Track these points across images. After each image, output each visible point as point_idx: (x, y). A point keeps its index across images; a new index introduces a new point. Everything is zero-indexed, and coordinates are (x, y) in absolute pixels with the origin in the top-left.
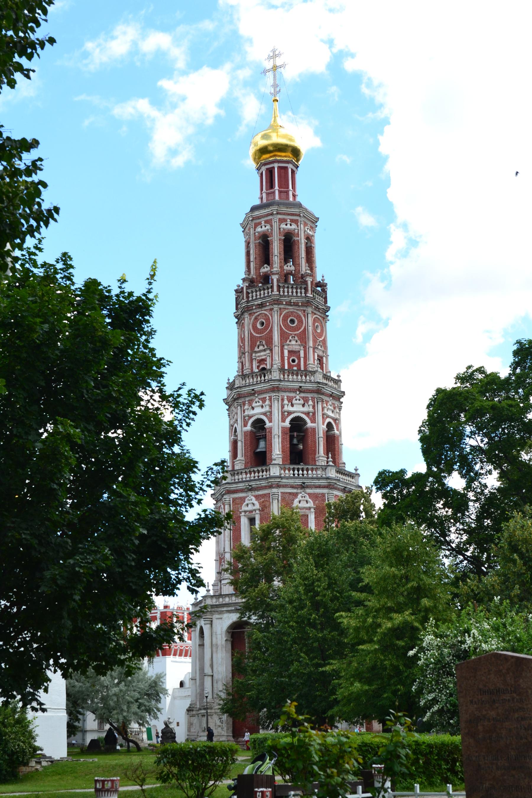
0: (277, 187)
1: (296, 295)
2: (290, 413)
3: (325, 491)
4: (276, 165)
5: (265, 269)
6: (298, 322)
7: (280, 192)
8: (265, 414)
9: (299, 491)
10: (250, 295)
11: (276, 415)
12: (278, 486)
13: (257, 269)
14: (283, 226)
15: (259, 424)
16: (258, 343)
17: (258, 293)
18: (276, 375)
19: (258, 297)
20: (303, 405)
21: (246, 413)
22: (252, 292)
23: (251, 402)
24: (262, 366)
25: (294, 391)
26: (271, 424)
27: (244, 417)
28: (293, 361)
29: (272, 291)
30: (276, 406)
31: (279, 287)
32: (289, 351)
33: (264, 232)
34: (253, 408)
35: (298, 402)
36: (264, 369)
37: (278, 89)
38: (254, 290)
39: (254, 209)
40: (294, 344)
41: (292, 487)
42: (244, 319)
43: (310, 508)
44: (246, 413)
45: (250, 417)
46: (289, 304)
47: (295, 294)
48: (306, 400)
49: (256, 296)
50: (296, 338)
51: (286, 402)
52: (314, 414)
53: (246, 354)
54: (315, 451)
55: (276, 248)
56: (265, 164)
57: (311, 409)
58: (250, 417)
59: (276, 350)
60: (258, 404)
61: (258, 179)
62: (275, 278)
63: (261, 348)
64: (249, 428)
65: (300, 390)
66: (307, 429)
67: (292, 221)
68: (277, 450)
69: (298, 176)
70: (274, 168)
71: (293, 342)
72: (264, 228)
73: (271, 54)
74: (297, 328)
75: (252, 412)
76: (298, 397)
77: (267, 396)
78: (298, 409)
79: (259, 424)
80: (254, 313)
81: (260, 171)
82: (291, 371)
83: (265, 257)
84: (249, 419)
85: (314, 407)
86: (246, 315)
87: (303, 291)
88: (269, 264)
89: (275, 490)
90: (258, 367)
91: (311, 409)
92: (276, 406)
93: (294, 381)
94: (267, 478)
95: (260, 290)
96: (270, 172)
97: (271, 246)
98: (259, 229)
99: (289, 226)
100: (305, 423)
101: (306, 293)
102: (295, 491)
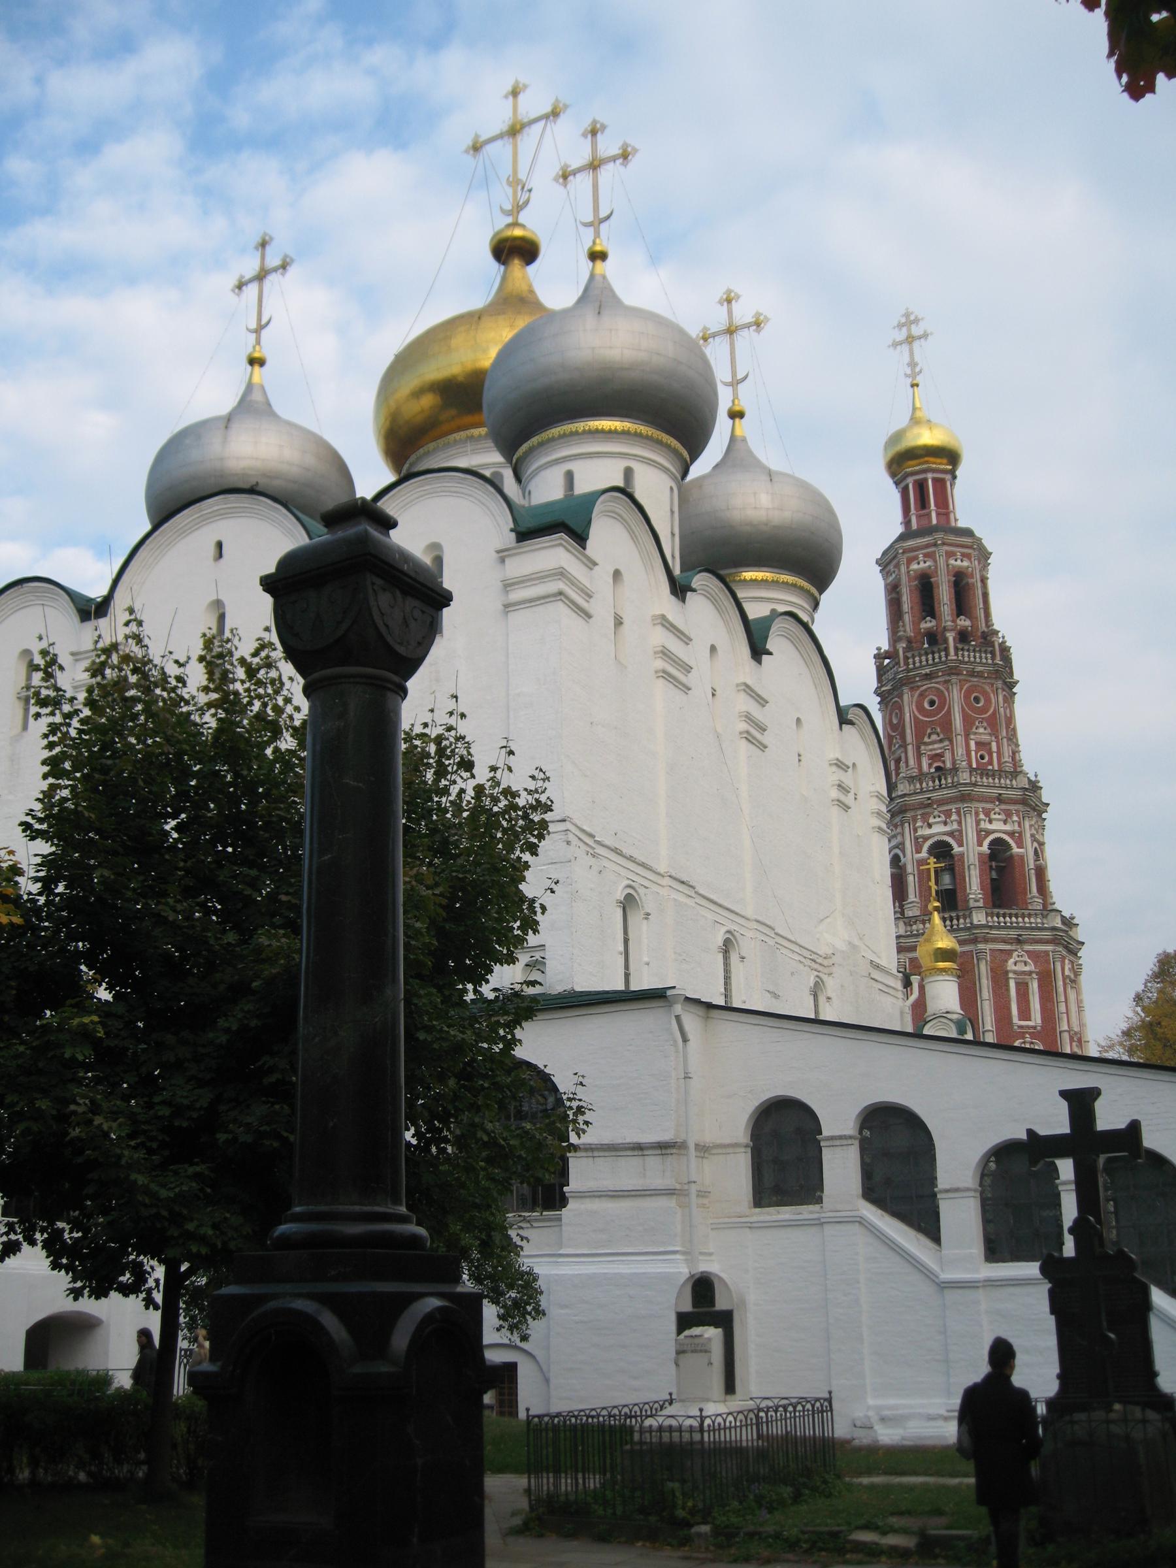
0: (933, 506)
1: (982, 661)
2: (989, 832)
3: (1049, 948)
4: (930, 476)
5: (928, 624)
6: (986, 701)
7: (938, 514)
8: (951, 834)
9: (1013, 948)
10: (911, 661)
11: (971, 835)
12: (986, 941)
13: (916, 624)
14: (952, 562)
15: (941, 850)
16: (929, 731)
17: (924, 658)
18: (964, 777)
19: (924, 663)
20: (1005, 822)
21: (920, 833)
22: (913, 656)
23: (925, 818)
24: (936, 765)
25: (990, 800)
26: (961, 849)
27: (916, 838)
28: (982, 757)
29: (947, 655)
30: (970, 822)
31: (956, 649)
32: (977, 743)
33: (922, 570)
34: (930, 826)
35: (997, 816)
36: (938, 769)
37: (917, 369)
38: (916, 653)
39: (902, 538)
40: (982, 732)
41: (1005, 941)
42: (901, 696)
43: (1030, 973)
44: (920, 833)
46: (972, 674)
47: (978, 660)
48: (1008, 814)
49: (921, 662)
50: (985, 724)
51: (982, 816)
52: (1020, 833)
53: (910, 747)
54: (1025, 889)
55: (944, 595)
57: (1016, 828)
58: (926, 838)
59: (960, 740)
60: (938, 819)
61: (895, 496)
62: (950, 636)
63: (934, 737)
65: (1000, 799)
66: (1012, 857)
67: (963, 555)
68: (974, 886)
69: (955, 491)
70: (926, 480)
71: (981, 730)
72: (922, 565)
73: (903, 320)
74: (984, 710)
75: (927, 832)
76: (997, 810)
77: (953, 807)
78: (998, 827)
79: (941, 850)
80: (919, 687)
81: (903, 485)
82: (983, 771)
83: (927, 605)
84: (924, 842)
85: (1020, 826)
86: (906, 690)
87: (989, 656)
88: (933, 616)
89: (981, 946)
90: (930, 765)
91: (1016, 828)
92: (970, 822)
93: (988, 787)
94: (968, 929)
95: (927, 654)
96: (921, 487)
97: (935, 591)
98: (914, 566)
99: (959, 562)
100: (1009, 847)
101: (993, 658)
102: (1008, 947)
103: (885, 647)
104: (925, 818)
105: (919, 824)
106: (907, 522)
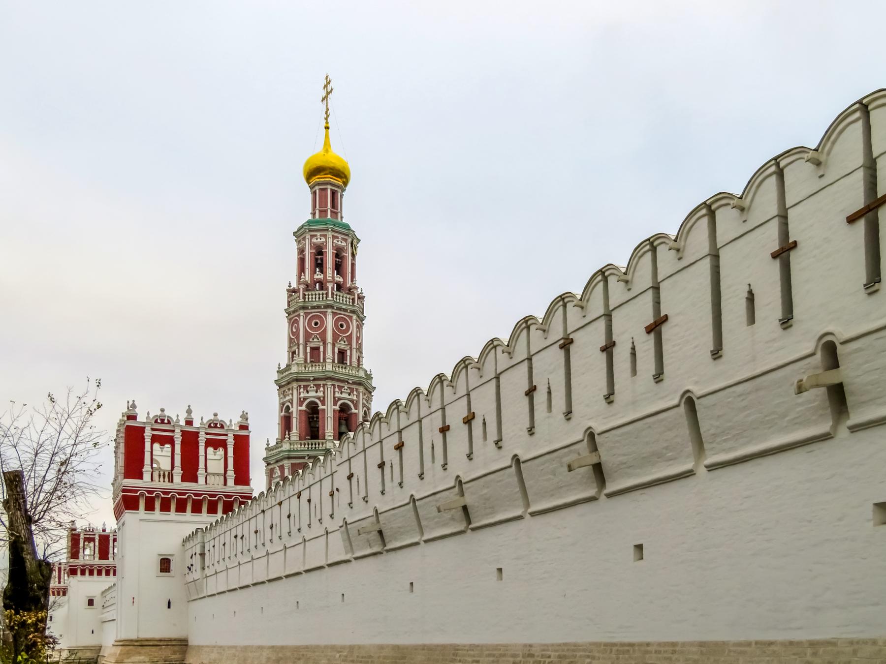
4: (329, 187)
7: (332, 212)
8: (319, 398)
34: (308, 392)
39: (309, 223)
44: (302, 395)
45: (305, 399)
51: (337, 390)
56: (319, 184)
61: (310, 197)
64: (303, 408)
67: (342, 239)
75: (307, 395)
77: (322, 383)
83: (319, 265)
98: (314, 240)
103: (294, 285)
104: (305, 387)
105: (302, 390)
106: (314, 214)
